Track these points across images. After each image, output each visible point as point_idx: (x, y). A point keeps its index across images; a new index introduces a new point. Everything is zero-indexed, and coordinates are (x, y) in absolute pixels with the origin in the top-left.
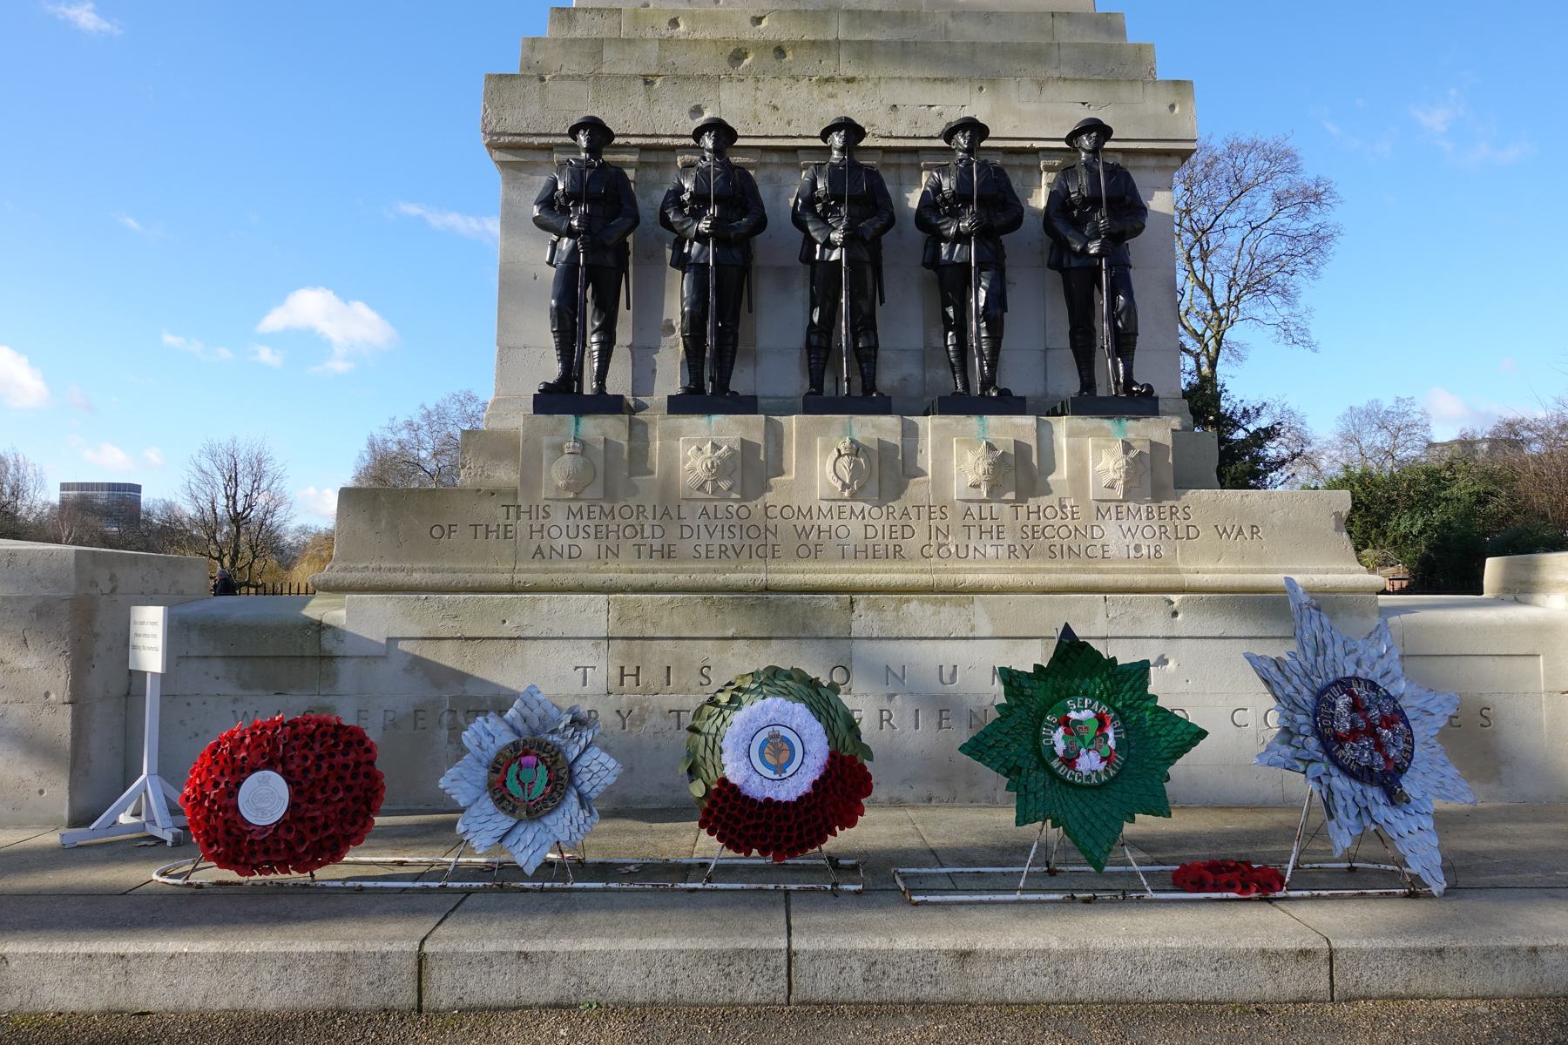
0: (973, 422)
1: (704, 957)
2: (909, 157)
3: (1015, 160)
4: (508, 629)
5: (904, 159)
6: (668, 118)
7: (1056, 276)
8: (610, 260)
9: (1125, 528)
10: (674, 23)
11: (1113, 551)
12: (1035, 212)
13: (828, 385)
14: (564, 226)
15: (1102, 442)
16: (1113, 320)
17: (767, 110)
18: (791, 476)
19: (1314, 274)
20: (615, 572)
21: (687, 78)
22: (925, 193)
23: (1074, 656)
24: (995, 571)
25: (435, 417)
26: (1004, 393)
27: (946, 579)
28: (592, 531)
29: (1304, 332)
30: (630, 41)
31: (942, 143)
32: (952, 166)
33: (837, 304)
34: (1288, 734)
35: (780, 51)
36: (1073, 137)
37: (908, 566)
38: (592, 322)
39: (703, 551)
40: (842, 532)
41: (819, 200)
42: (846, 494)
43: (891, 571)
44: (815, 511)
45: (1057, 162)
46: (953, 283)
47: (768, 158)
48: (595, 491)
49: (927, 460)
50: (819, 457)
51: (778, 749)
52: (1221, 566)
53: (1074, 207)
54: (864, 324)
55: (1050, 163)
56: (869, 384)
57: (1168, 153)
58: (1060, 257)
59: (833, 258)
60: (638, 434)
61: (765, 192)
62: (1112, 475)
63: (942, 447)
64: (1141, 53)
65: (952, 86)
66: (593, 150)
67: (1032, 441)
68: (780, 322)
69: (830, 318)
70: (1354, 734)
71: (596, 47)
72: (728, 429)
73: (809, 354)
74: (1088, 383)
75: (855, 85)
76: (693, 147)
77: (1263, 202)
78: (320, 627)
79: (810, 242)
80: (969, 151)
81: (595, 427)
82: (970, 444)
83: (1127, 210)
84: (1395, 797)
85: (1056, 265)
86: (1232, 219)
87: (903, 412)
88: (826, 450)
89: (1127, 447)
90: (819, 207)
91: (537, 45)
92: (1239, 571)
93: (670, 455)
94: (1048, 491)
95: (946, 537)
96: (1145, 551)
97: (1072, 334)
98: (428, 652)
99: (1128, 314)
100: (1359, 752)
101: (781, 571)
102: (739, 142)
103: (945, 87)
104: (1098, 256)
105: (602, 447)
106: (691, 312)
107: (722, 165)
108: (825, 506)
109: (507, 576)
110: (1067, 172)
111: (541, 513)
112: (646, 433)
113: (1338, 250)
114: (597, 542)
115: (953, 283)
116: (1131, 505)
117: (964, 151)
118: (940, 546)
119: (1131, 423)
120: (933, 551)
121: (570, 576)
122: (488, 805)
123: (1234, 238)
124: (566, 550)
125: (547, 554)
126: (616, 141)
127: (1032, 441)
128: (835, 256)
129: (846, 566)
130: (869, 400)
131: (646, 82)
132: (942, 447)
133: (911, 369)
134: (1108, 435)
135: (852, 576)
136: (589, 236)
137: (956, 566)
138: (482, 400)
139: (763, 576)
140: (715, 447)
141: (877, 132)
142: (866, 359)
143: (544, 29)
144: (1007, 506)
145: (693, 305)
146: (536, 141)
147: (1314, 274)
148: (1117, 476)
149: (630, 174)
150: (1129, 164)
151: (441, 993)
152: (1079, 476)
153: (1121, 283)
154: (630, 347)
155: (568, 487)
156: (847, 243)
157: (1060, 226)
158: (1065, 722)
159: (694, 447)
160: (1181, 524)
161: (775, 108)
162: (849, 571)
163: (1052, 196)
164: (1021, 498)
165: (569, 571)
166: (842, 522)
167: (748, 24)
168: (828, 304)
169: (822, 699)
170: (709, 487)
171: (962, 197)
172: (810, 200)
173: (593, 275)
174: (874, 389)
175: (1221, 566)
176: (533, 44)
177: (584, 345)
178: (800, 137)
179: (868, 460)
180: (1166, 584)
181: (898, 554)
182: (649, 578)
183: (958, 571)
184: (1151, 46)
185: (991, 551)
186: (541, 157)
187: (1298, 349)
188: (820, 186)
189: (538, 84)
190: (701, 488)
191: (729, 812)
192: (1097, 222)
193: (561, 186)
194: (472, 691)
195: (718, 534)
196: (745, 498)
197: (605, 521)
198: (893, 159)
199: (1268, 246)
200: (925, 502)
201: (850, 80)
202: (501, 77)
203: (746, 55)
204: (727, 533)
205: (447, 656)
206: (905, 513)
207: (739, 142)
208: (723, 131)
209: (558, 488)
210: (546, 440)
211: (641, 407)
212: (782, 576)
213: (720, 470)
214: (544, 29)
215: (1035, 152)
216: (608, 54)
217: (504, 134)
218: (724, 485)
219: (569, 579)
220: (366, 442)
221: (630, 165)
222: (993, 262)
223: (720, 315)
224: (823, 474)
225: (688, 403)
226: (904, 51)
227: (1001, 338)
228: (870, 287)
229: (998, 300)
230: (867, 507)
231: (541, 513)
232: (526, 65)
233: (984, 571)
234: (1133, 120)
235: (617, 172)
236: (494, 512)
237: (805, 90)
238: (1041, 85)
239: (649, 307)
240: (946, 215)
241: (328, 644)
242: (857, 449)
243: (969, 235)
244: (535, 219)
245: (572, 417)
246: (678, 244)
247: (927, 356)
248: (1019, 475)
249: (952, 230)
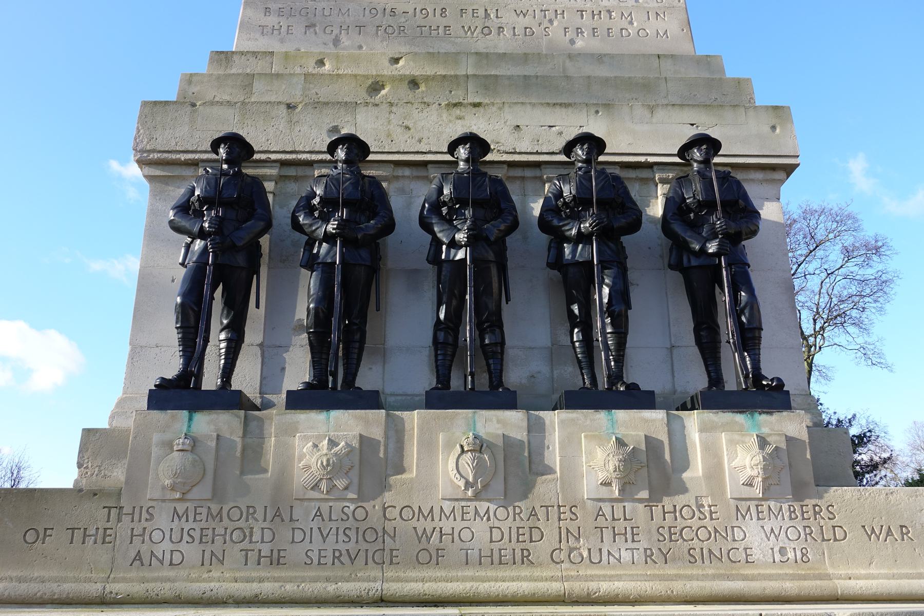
0: (602, 416)
2: (534, 168)
3: (632, 174)
5: (528, 173)
7: (677, 276)
8: (240, 260)
9: (768, 530)
10: (321, 63)
12: (653, 220)
13: (456, 383)
14: (196, 229)
15: (736, 437)
16: (736, 313)
17: (399, 130)
18: (412, 474)
19: (881, 310)
21: (326, 104)
22: (547, 200)
24: (633, 578)
26: (633, 388)
27: (578, 587)
28: (196, 535)
29: (880, 355)
30: (278, 75)
31: (563, 158)
32: (572, 174)
33: (465, 300)
35: (414, 83)
36: (684, 151)
37: (537, 573)
38: (218, 319)
39: (315, 556)
40: (466, 535)
41: (445, 204)
42: (470, 493)
43: (518, 579)
44: (436, 511)
45: (671, 175)
47: (400, 172)
48: (203, 491)
49: (554, 456)
50: (442, 452)
52: (873, 571)
53: (689, 209)
54: (491, 322)
55: (664, 175)
56: (496, 379)
57: (773, 168)
59: (457, 258)
61: (396, 202)
62: (749, 472)
63: (570, 442)
64: (741, 86)
65: (570, 110)
67: (663, 437)
68: (408, 322)
69: (455, 317)
71: (248, 81)
72: (347, 425)
73: (436, 350)
74: (716, 379)
75: (481, 109)
76: (330, 162)
77: (833, 255)
79: (437, 243)
80: (587, 161)
81: (206, 423)
82: (600, 439)
83: (742, 216)
85: (676, 266)
86: (811, 268)
87: (528, 408)
88: (449, 446)
89: (763, 442)
90: (444, 210)
91: (194, 79)
92: (893, 577)
94: (684, 490)
95: (577, 539)
96: (791, 555)
97: (697, 331)
99: (752, 309)
101: (398, 580)
102: (371, 157)
103: (564, 110)
104: (717, 255)
105: (214, 444)
106: (316, 309)
107: (352, 172)
108: (447, 506)
109: (99, 586)
110: (682, 181)
111: (145, 515)
112: (261, 428)
113: (898, 290)
114: (202, 547)
115: (575, 282)
116: (772, 504)
117: (583, 161)
118: (571, 550)
119: (764, 417)
120: (564, 555)
121: (168, 585)
123: (813, 283)
124: (168, 556)
125: (146, 561)
126: (256, 157)
127: (663, 437)
128: (460, 255)
129: (469, 573)
130: (499, 397)
132: (570, 442)
134: (741, 429)
135: (475, 584)
136: (218, 236)
137: (589, 572)
139: (378, 585)
140: (332, 443)
141: (502, 148)
142: (493, 355)
143: (201, 66)
144: (641, 506)
145: (318, 302)
146: (183, 157)
147: (881, 310)
148: (755, 473)
149: (269, 186)
150: (739, 176)
152: (715, 473)
153: (741, 280)
154: (261, 345)
155: (173, 488)
156: (472, 242)
157: (677, 228)
159: (312, 443)
160: (827, 525)
161: (407, 128)
162: (473, 579)
163: (668, 202)
164: (655, 497)
165: (168, 580)
166: (465, 524)
167: (387, 63)
168: (454, 303)
170: (324, 486)
171: (582, 202)
172: (436, 205)
173: (222, 274)
174: (500, 383)
175: (873, 571)
176: (189, 79)
177: (206, 341)
178: (430, 152)
179: (493, 457)
180: (817, 593)
181: (526, 559)
183: (591, 578)
184: (748, 81)
185: (626, 556)
188: (446, 191)
189: (189, 108)
190: (315, 487)
192: (714, 224)
193: (197, 193)
195: (332, 538)
196: (362, 497)
197: (212, 524)
198: (518, 172)
199: (843, 288)
200: (554, 501)
201: (476, 105)
202: (155, 103)
203: (383, 87)
204: (341, 537)
206: (533, 514)
207: (371, 157)
208: (357, 148)
209: (164, 488)
210: (156, 438)
211: (267, 405)
212: (399, 585)
213: (335, 468)
214: (201, 66)
215: (650, 166)
217: (154, 151)
218: (340, 483)
219: (166, 589)
221: (269, 178)
222: (616, 261)
223: (347, 312)
224: (446, 472)
225: (313, 397)
226: (526, 84)
227: (625, 334)
228: (495, 285)
229: (621, 296)
230: (493, 507)
231: (145, 515)
232: (183, 93)
233: (619, 578)
234: (739, 143)
235: (256, 183)
237: (434, 117)
238: (652, 109)
240: (568, 217)
242: (480, 446)
243: (590, 235)
244: (171, 222)
245: (185, 413)
246: (310, 244)
248: (652, 472)
249: (574, 232)
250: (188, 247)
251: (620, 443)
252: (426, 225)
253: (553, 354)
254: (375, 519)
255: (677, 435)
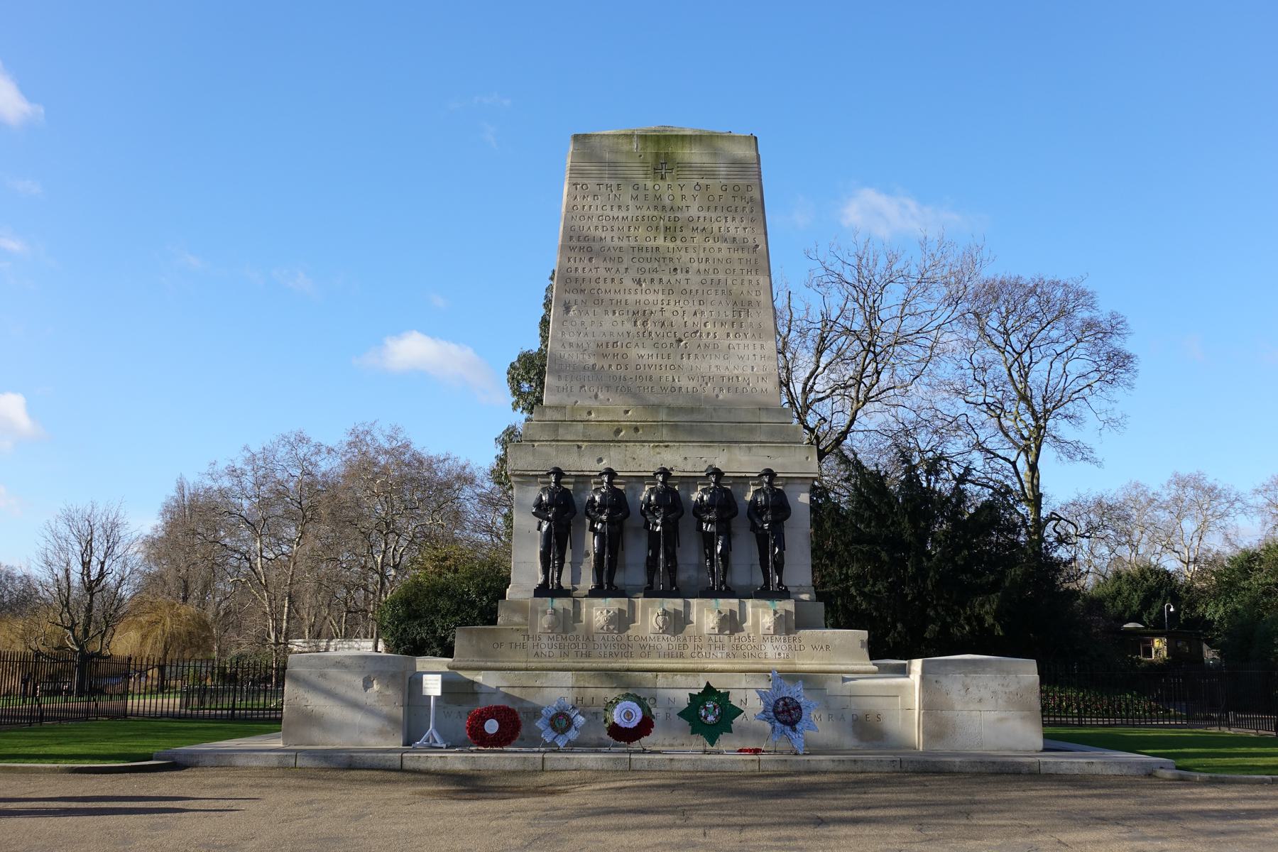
0: (713, 601)
1: (610, 759)
2: (690, 481)
4: (538, 684)
6: (588, 463)
7: (753, 535)
10: (590, 413)
11: (769, 655)
18: (639, 623)
20: (568, 663)
23: (709, 689)
25: (262, 463)
26: (727, 588)
27: (700, 666)
34: (764, 712)
46: (709, 541)
48: (560, 629)
49: (694, 617)
50: (651, 615)
51: (629, 715)
54: (671, 557)
56: (673, 583)
58: (754, 528)
60: (576, 605)
61: (629, 496)
63: (700, 611)
66: (557, 482)
68: (636, 552)
69: (656, 555)
70: (783, 712)
72: (613, 604)
74: (767, 583)
78: (473, 682)
81: (561, 603)
82: (712, 611)
84: (794, 730)
88: (653, 613)
89: (775, 612)
93: (589, 614)
98: (510, 691)
100: (784, 717)
115: (709, 541)
122: (550, 729)
131: (579, 447)
132: (700, 611)
133: (693, 573)
138: (314, 441)
142: (672, 570)
151: (548, 765)
152: (756, 624)
153: (780, 542)
158: (706, 708)
159: (599, 612)
164: (732, 633)
169: (640, 702)
181: (682, 656)
182: (581, 665)
186: (533, 479)
187: (1087, 464)
188: (653, 498)
191: (618, 733)
194: (525, 705)
196: (620, 632)
205: (516, 693)
208: (611, 473)
211: (575, 589)
213: (610, 621)
216: (561, 431)
219: (549, 665)
220: (174, 486)
225: (596, 593)
236: (518, 638)
239: (580, 554)
241: (476, 688)
242: (665, 613)
247: (700, 567)
248: (731, 624)
250: (540, 524)
251: (720, 612)
252: (643, 513)
253: (700, 567)
254: (625, 641)
255: (742, 607)
